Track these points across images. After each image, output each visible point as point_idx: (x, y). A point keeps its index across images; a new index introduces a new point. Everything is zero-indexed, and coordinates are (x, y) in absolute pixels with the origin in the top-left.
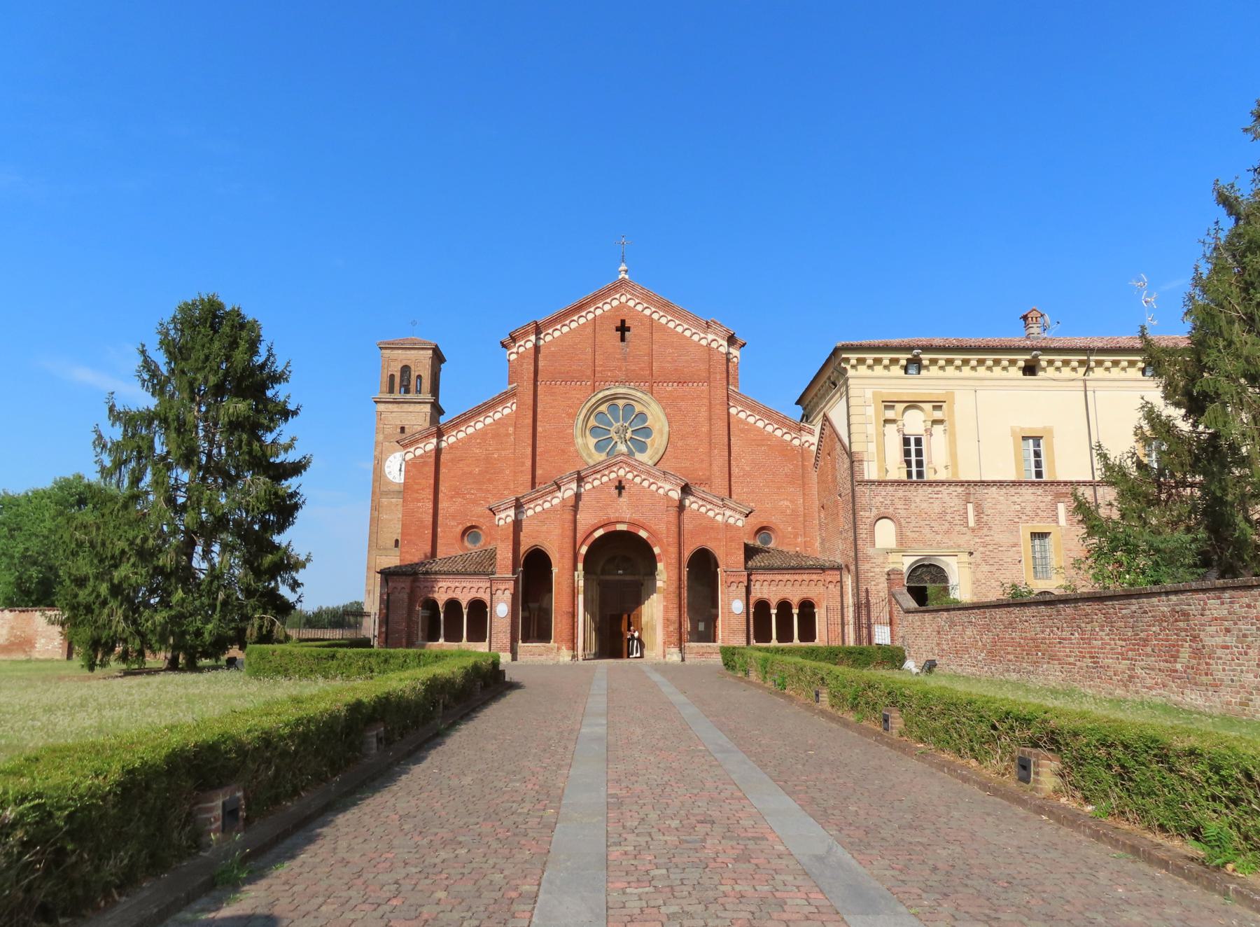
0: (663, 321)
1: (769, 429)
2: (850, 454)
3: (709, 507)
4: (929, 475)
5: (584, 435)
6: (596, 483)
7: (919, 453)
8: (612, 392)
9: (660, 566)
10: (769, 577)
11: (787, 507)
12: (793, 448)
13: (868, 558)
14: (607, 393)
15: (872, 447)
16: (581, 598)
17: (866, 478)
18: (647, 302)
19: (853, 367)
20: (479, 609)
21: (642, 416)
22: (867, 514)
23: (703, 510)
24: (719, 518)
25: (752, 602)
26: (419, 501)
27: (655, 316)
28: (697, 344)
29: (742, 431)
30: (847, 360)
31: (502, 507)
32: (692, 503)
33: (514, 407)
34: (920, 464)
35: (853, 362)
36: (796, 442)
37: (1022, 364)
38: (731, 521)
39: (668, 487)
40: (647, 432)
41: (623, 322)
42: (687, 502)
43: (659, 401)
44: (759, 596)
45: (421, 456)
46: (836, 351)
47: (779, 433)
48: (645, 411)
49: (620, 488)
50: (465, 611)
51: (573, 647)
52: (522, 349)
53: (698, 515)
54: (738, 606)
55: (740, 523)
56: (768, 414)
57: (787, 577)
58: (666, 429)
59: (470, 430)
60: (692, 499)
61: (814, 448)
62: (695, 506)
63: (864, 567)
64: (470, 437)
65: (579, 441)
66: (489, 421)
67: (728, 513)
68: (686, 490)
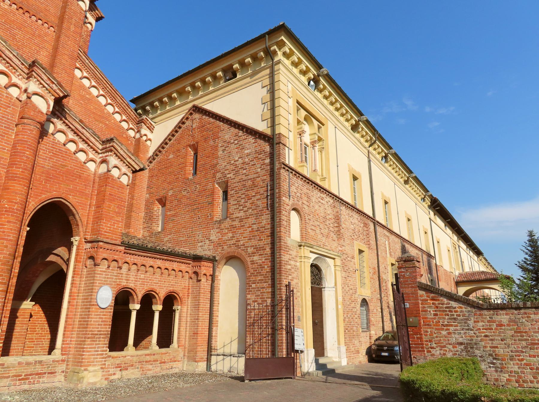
3: (82, 145)
10: (139, 260)
23: (72, 147)
24: (91, 166)
29: (83, 97)
32: (59, 133)
38: (115, 173)
42: (51, 129)
44: (124, 283)
46: (282, 28)
47: (118, 117)
53: (60, 151)
56: (112, 93)
57: (159, 263)
60: (60, 125)
62: (61, 138)
67: (113, 160)
68: (59, 109)
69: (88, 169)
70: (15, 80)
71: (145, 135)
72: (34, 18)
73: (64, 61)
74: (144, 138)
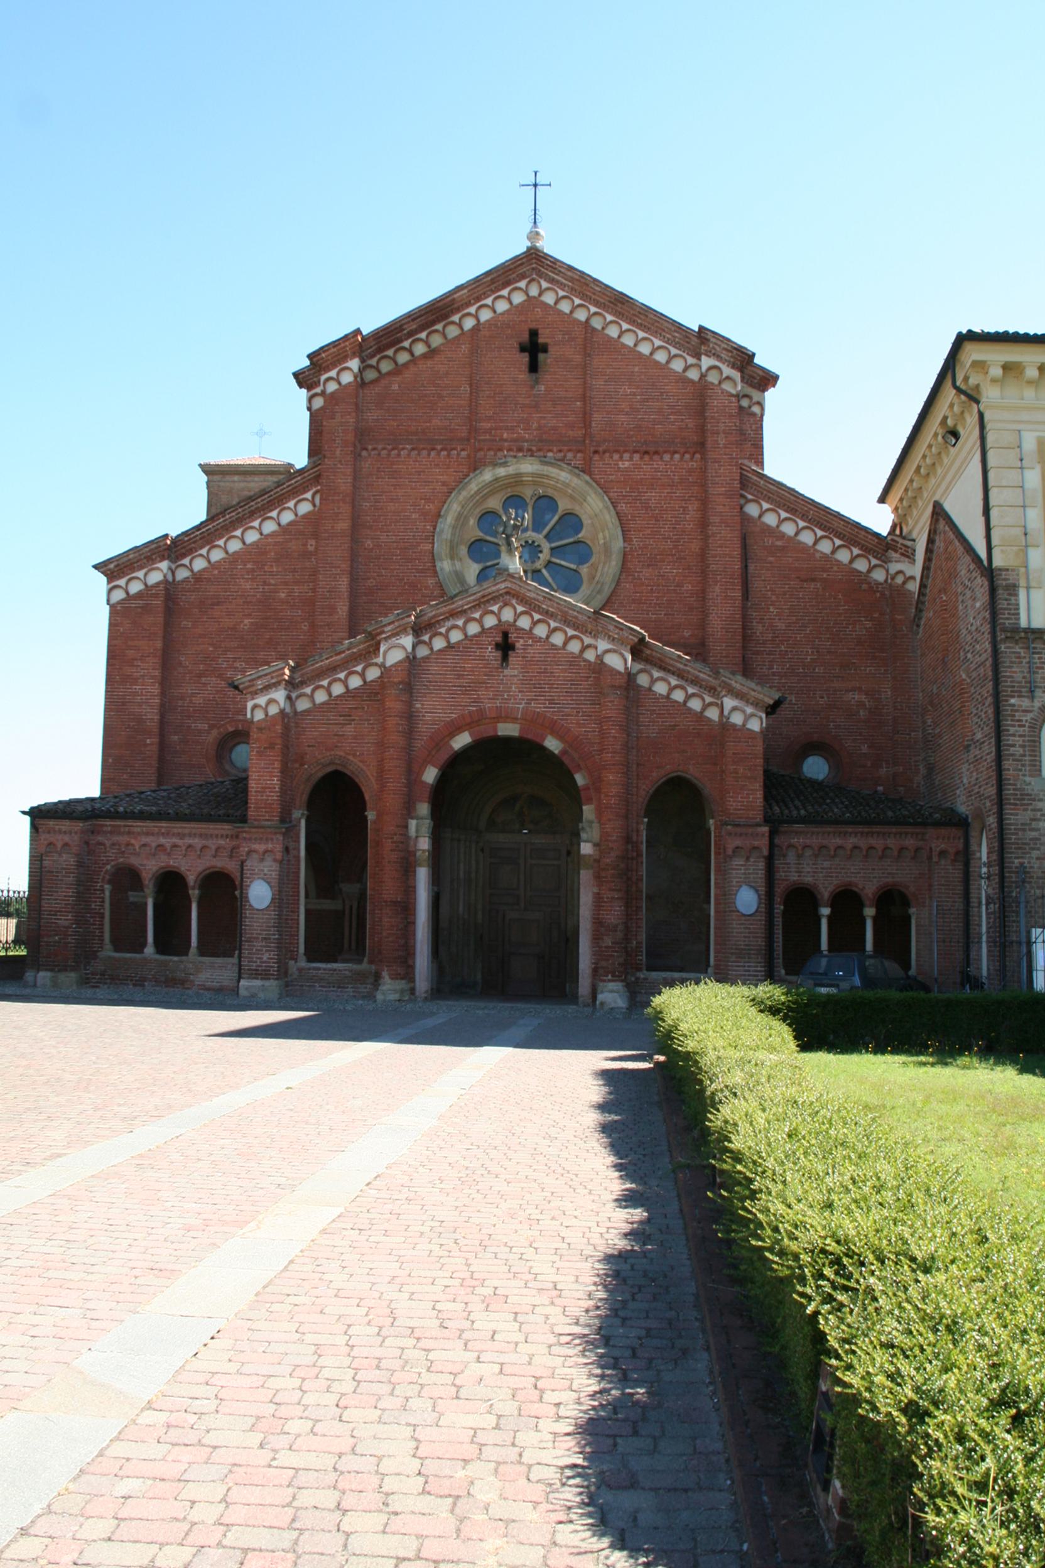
0: (613, 331)
1: (825, 547)
2: (990, 573)
5: (453, 556)
6: (456, 636)
9: (588, 811)
11: (861, 704)
12: (873, 587)
13: (1026, 799)
14: (501, 472)
17: (1023, 623)
18: (582, 296)
20: (223, 890)
21: (571, 521)
22: (1025, 703)
24: (713, 714)
25: (779, 890)
26: (135, 681)
27: (597, 323)
28: (682, 379)
31: (260, 684)
35: (996, 372)
36: (879, 576)
38: (737, 719)
39: (603, 645)
40: (582, 551)
41: (534, 334)
43: (604, 489)
44: (794, 877)
45: (139, 595)
48: (577, 509)
49: (505, 647)
50: (194, 893)
51: (407, 973)
52: (332, 387)
54: (747, 900)
55: (755, 725)
58: (618, 544)
59: (234, 546)
61: (913, 587)
63: (1016, 817)
64: (233, 559)
65: (445, 566)
66: (269, 527)
67: (729, 703)
69: (709, 720)
70: (588, 641)
71: (900, 572)
72: (667, 457)
73: (720, 508)
74: (899, 580)
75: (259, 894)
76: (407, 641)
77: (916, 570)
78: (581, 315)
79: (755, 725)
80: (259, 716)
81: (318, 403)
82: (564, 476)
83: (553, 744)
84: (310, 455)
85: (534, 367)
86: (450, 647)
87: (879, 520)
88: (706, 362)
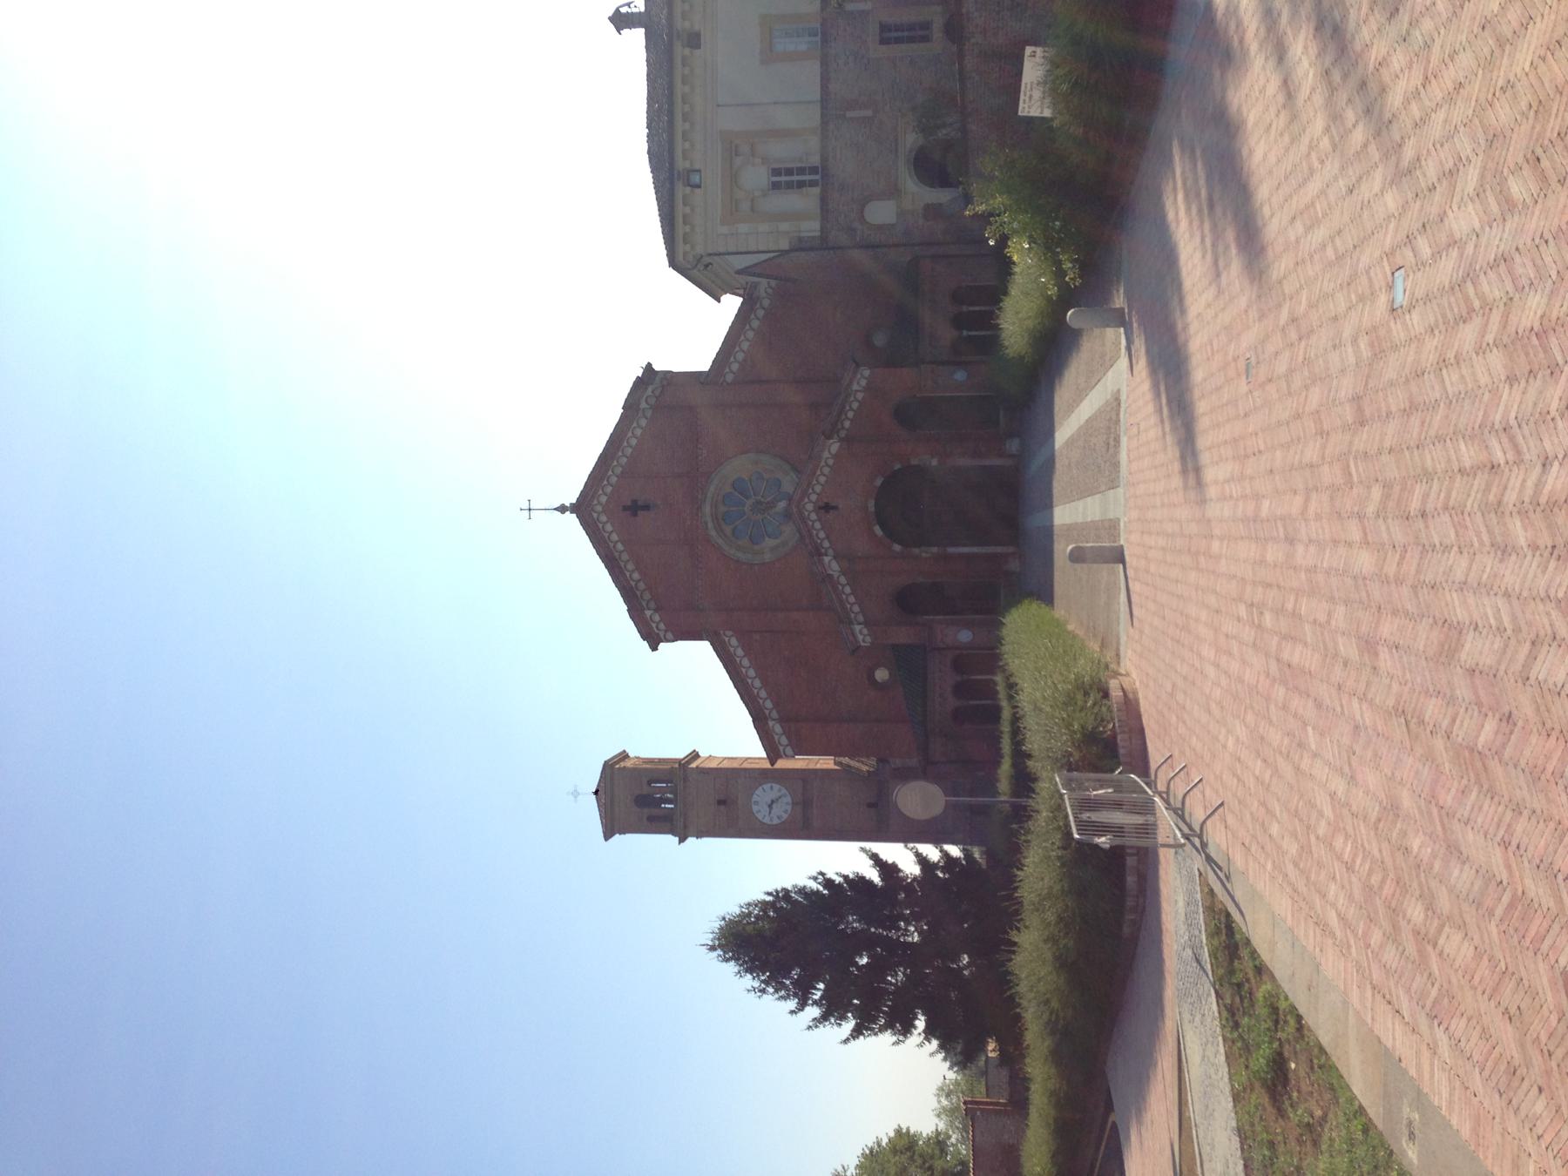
4: (815, 160)
6: (822, 535)
7: (789, 172)
8: (709, 519)
9: (914, 462)
14: (710, 525)
15: (784, 226)
16: (951, 550)
19: (693, 247)
24: (860, 396)
30: (685, 254)
33: (729, 633)
34: (801, 171)
35: (688, 248)
36: (766, 303)
37: (687, 51)
38: (864, 382)
39: (826, 454)
41: (625, 508)
45: (789, 738)
52: (662, 626)
59: (757, 683)
61: (773, 283)
64: (765, 684)
65: (768, 557)
66: (746, 662)
67: (855, 387)
75: (965, 636)
76: (827, 559)
77: (764, 282)
78: (614, 479)
79: (867, 373)
80: (868, 639)
81: (670, 635)
82: (712, 489)
83: (879, 482)
84: (701, 639)
85: (646, 507)
86: (828, 537)
87: (732, 304)
88: (643, 405)
